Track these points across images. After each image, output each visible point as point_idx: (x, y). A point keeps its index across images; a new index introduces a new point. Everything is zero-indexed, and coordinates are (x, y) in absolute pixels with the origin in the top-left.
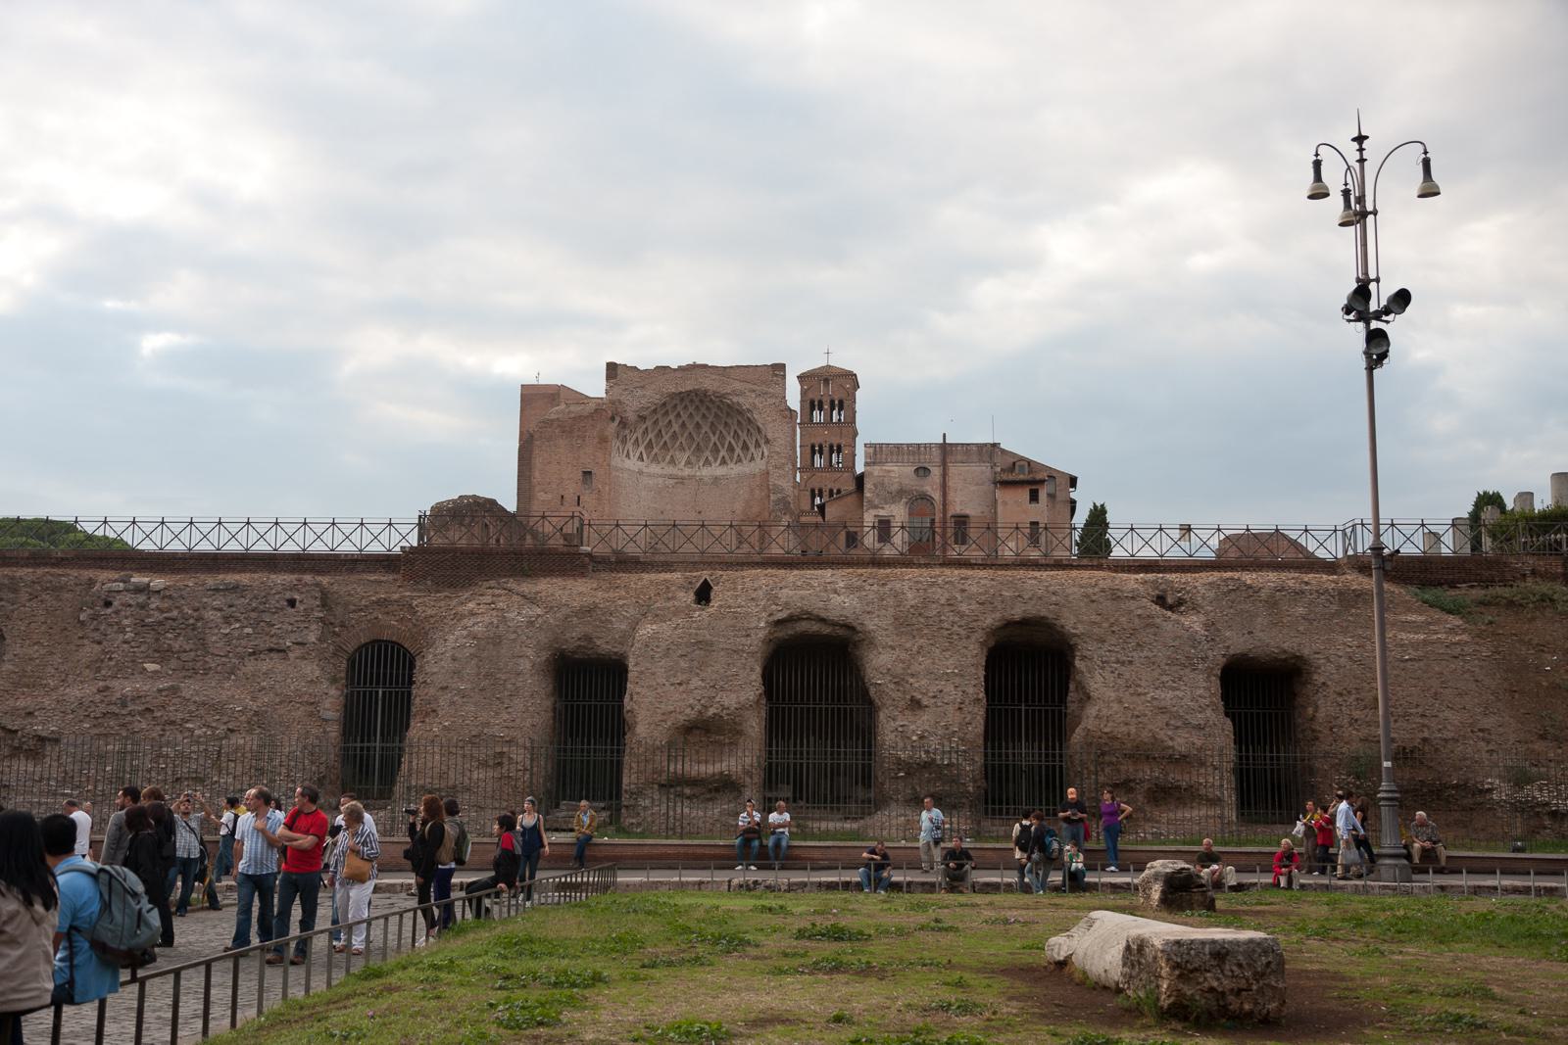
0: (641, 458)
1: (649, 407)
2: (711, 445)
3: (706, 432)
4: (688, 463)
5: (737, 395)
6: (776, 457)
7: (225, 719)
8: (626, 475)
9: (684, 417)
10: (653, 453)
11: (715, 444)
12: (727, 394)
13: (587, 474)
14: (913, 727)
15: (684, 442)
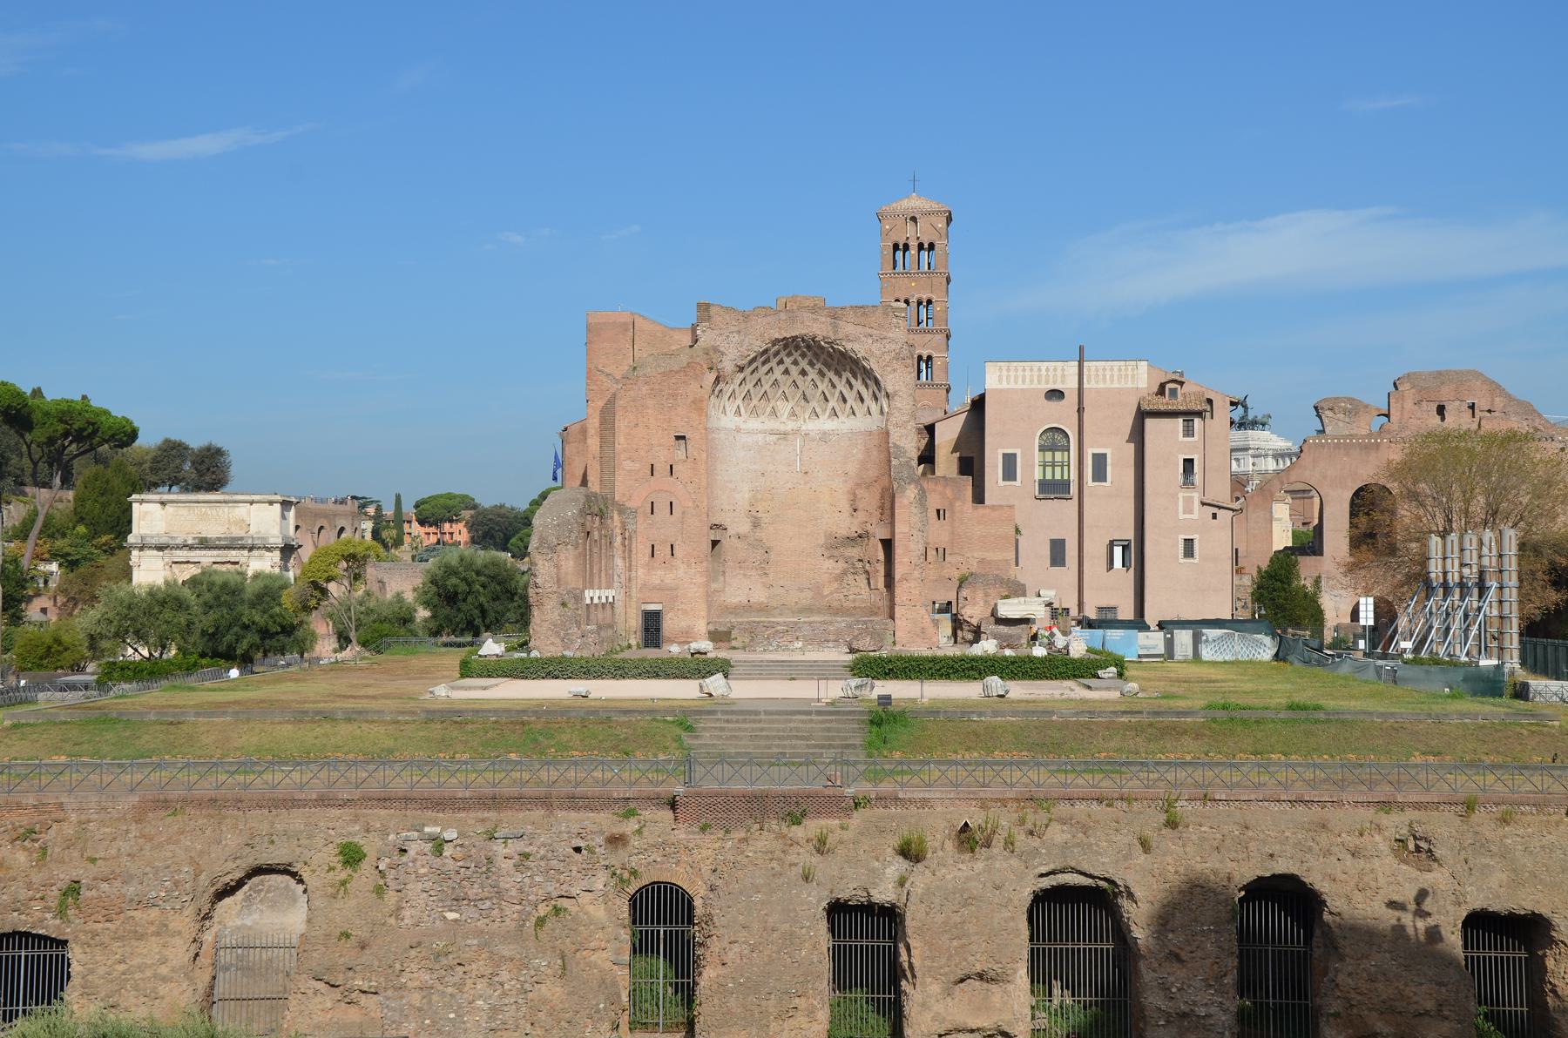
0: (738, 412)
2: (819, 394)
4: (793, 414)
6: (897, 414)
7: (533, 973)
8: (722, 436)
9: (788, 361)
10: (752, 405)
14: (1171, 979)
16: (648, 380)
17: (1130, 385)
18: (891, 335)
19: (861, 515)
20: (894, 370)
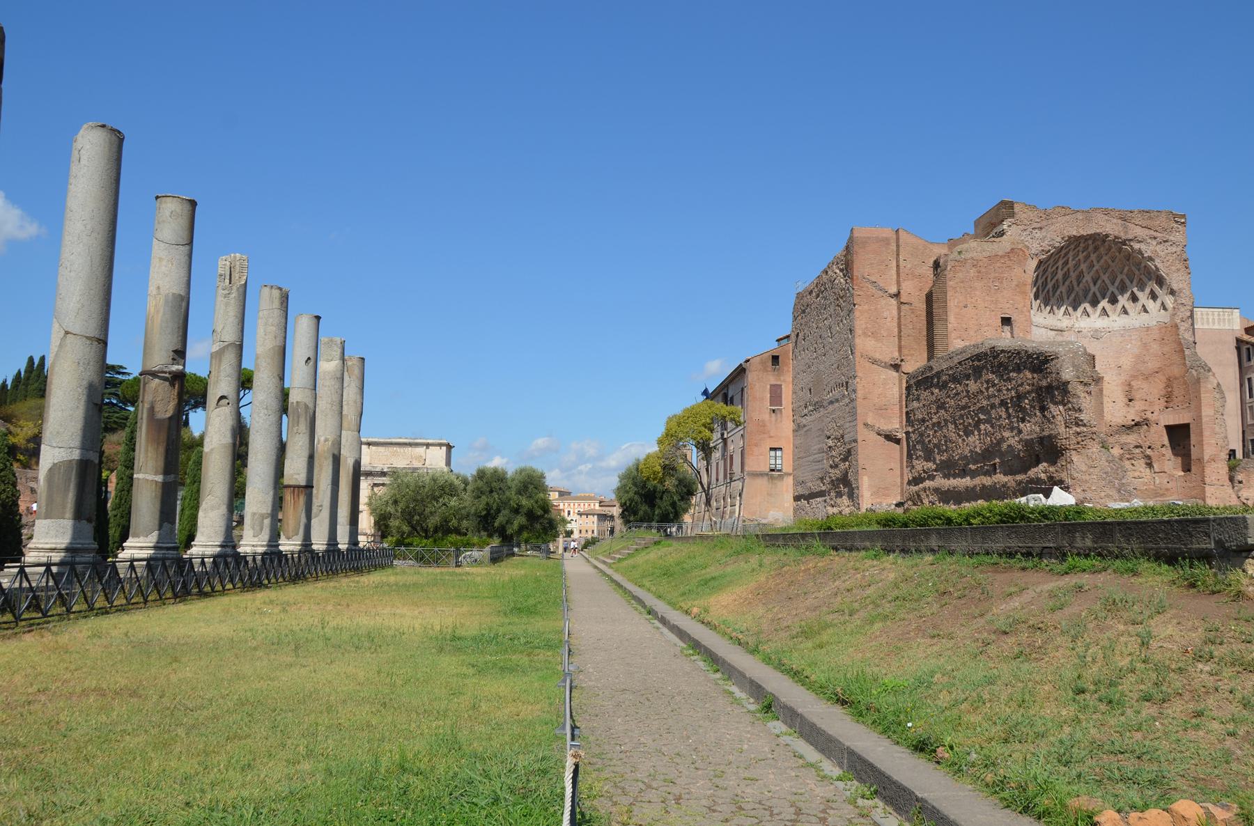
1: (1049, 251)
3: (1087, 281)
5: (1140, 242)
6: (1182, 309)
9: (1071, 264)
11: (1094, 293)
12: (1131, 240)
13: (1006, 321)
15: (1063, 291)
16: (975, 263)
17: (1227, 327)
18: (1171, 238)
19: (1138, 405)
20: (1178, 270)
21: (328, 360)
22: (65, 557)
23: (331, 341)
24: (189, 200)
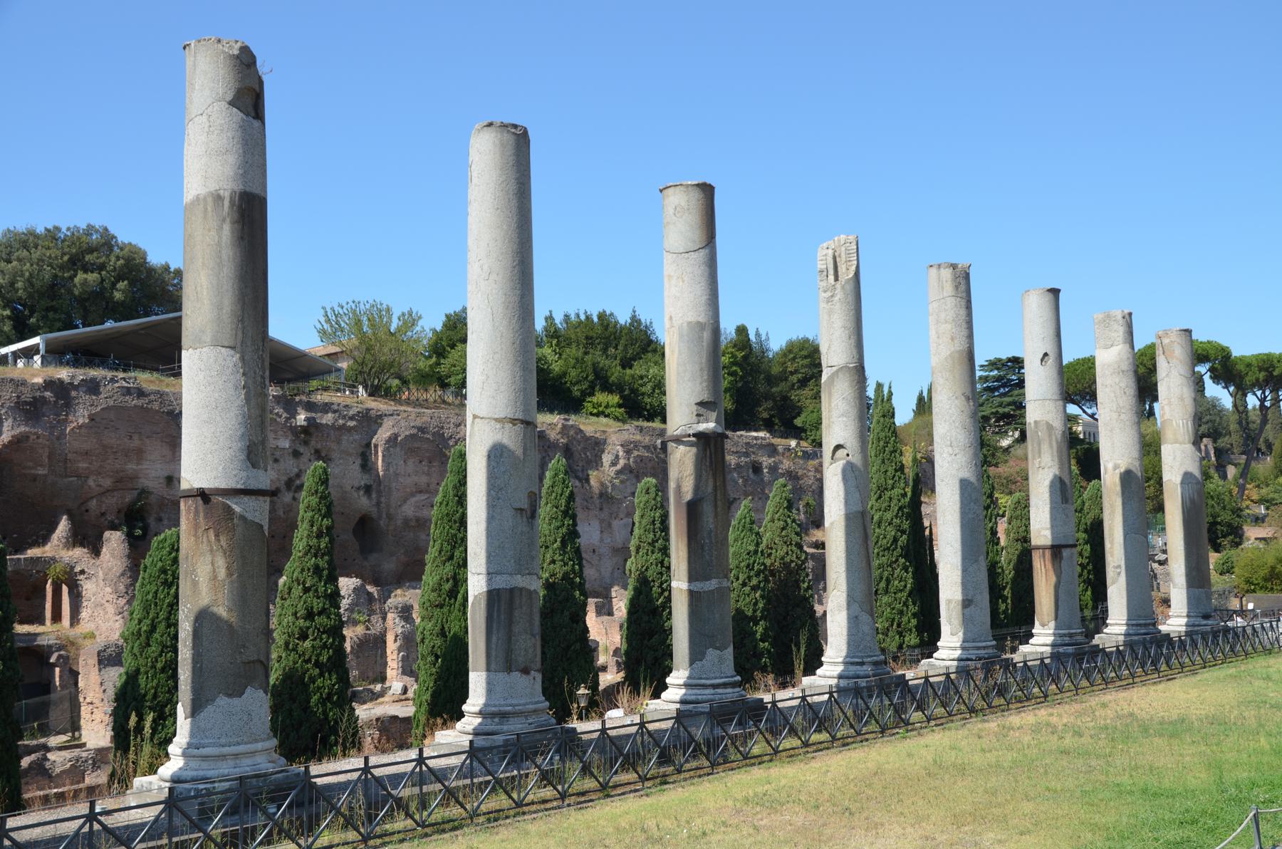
21: (1107, 347)
22: (480, 724)
23: (1108, 316)
24: (698, 185)
